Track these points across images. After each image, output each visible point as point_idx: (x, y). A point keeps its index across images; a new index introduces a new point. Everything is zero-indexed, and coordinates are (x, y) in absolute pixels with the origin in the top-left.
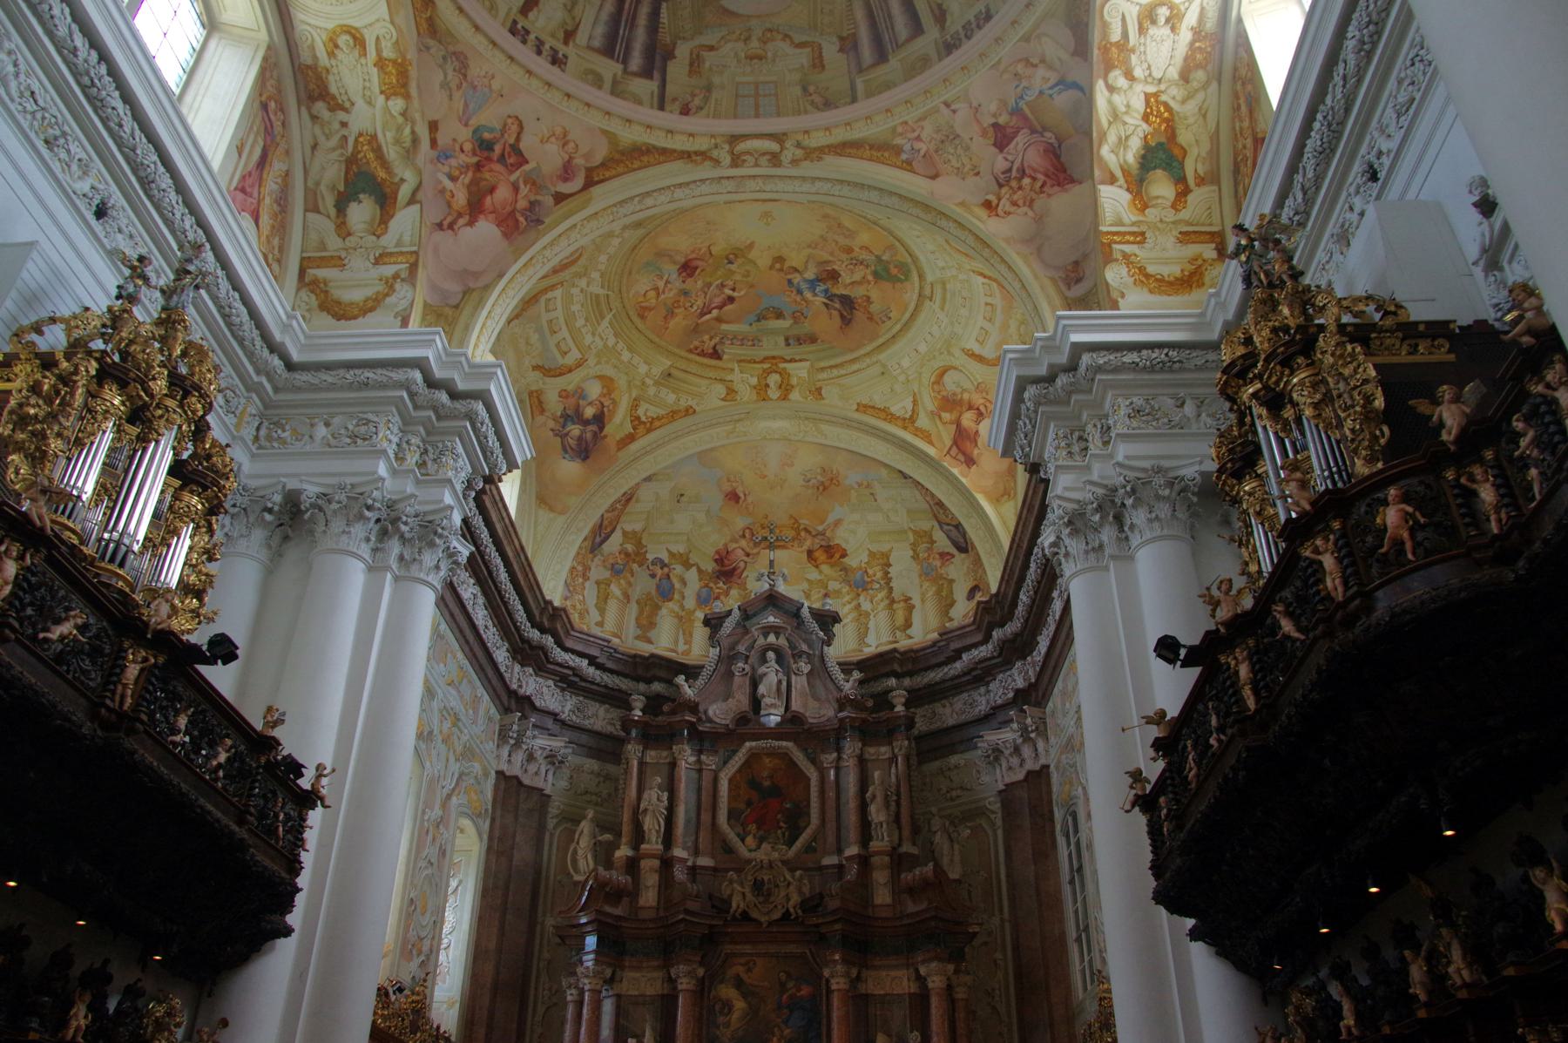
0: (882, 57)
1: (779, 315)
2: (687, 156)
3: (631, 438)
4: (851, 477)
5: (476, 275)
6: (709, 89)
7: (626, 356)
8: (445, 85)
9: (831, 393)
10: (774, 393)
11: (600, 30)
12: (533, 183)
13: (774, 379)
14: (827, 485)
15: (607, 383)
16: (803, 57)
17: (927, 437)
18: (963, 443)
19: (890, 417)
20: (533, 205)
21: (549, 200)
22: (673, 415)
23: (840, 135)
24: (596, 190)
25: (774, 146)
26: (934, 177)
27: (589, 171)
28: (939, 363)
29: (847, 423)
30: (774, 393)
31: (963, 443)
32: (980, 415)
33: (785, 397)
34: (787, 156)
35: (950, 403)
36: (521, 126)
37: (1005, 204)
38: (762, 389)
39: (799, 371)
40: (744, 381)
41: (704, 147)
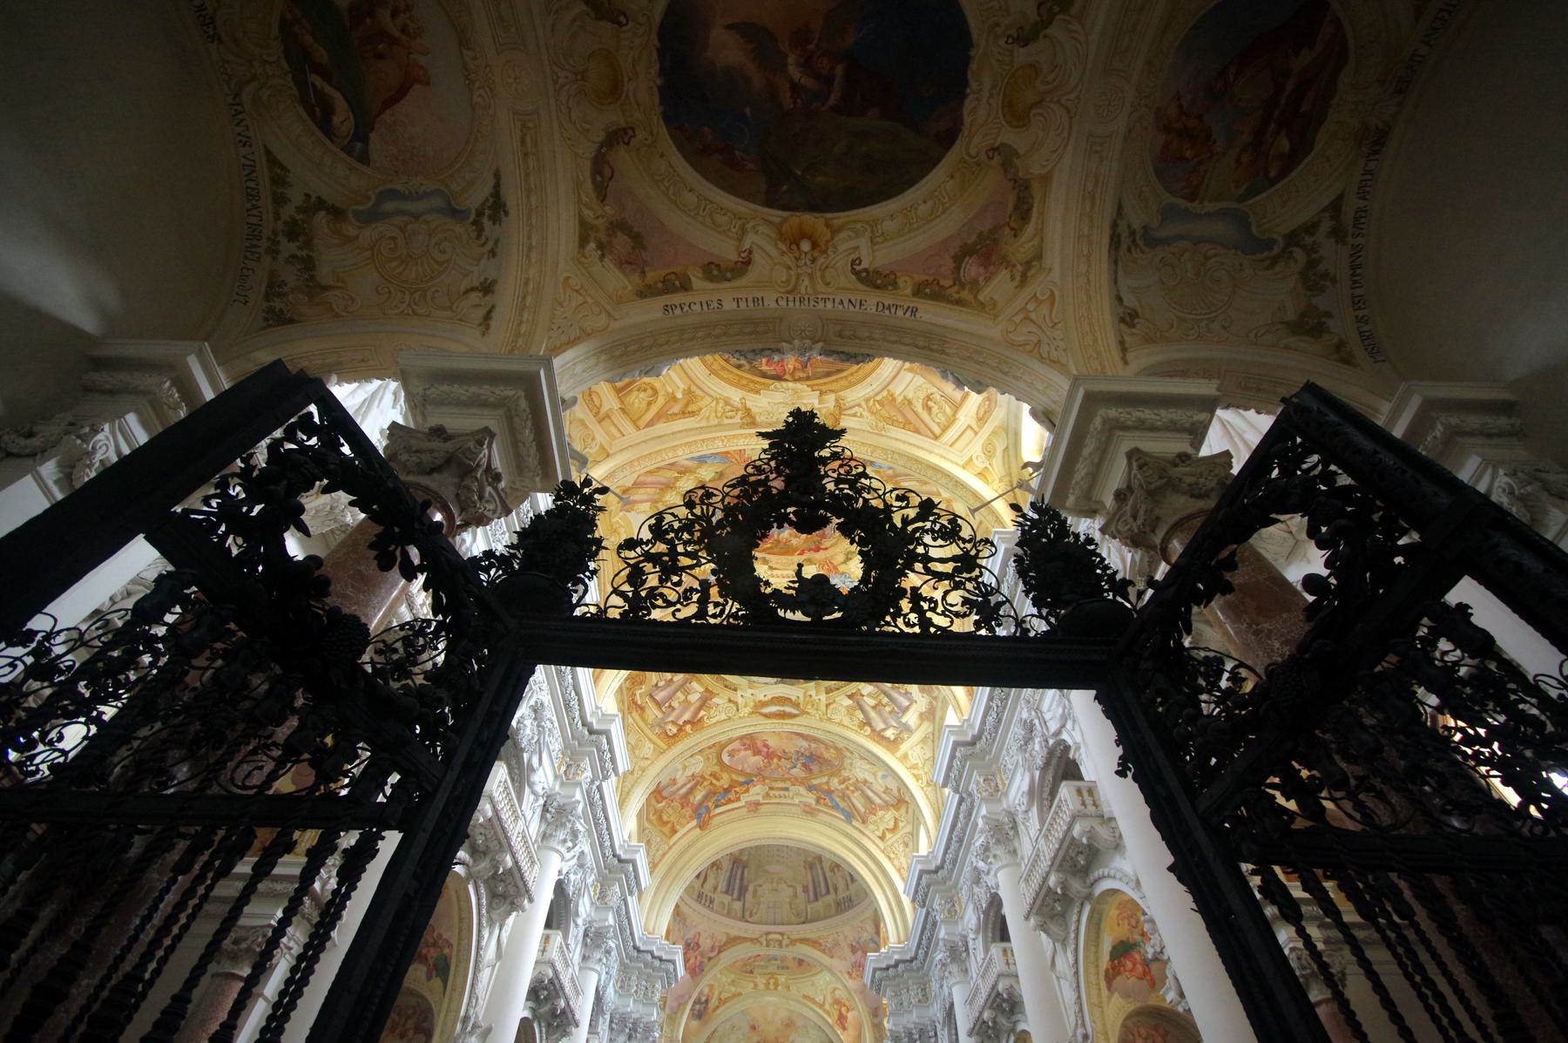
0: (816, 899)
1: (776, 960)
2: (751, 940)
3: (718, 1007)
4: (800, 1023)
5: (682, 996)
6: (759, 904)
7: (719, 976)
8: (679, 930)
9: (793, 989)
10: (772, 987)
11: (725, 884)
12: (702, 955)
13: (772, 981)
14: (789, 1024)
15: (711, 987)
16: (790, 892)
17: (828, 1013)
18: (842, 1019)
19: (815, 1002)
20: (701, 963)
21: (706, 960)
22: (734, 996)
23: (802, 936)
24: (722, 955)
25: (779, 937)
26: (832, 957)
27: (720, 947)
28: (834, 985)
29: (798, 1002)
30: (772, 987)
31: (842, 1019)
32: (848, 1010)
33: (776, 989)
34: (784, 943)
35: (837, 1002)
36: (699, 934)
37: (854, 975)
38: (768, 984)
39: (782, 979)
40: (761, 981)
41: (757, 936)
